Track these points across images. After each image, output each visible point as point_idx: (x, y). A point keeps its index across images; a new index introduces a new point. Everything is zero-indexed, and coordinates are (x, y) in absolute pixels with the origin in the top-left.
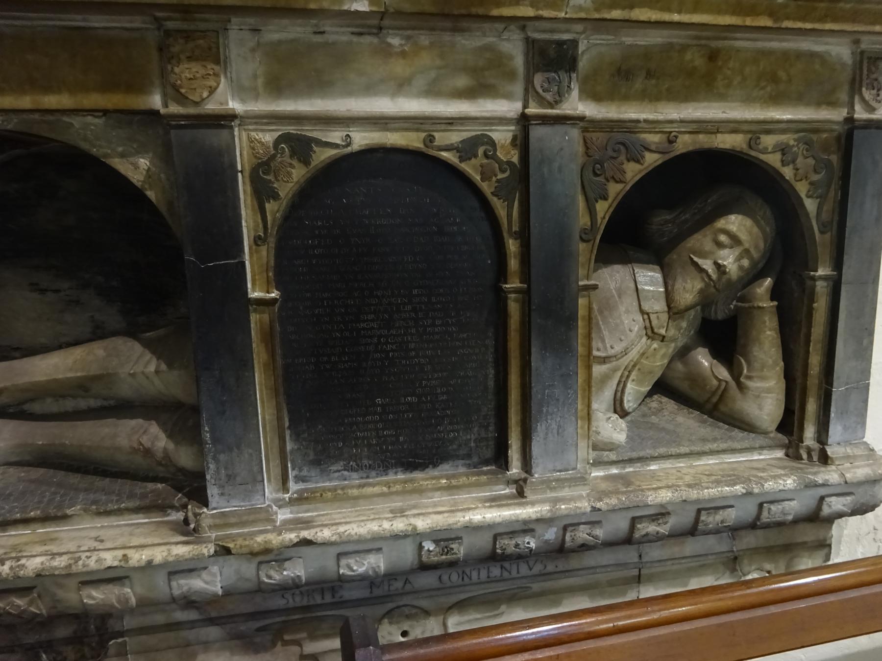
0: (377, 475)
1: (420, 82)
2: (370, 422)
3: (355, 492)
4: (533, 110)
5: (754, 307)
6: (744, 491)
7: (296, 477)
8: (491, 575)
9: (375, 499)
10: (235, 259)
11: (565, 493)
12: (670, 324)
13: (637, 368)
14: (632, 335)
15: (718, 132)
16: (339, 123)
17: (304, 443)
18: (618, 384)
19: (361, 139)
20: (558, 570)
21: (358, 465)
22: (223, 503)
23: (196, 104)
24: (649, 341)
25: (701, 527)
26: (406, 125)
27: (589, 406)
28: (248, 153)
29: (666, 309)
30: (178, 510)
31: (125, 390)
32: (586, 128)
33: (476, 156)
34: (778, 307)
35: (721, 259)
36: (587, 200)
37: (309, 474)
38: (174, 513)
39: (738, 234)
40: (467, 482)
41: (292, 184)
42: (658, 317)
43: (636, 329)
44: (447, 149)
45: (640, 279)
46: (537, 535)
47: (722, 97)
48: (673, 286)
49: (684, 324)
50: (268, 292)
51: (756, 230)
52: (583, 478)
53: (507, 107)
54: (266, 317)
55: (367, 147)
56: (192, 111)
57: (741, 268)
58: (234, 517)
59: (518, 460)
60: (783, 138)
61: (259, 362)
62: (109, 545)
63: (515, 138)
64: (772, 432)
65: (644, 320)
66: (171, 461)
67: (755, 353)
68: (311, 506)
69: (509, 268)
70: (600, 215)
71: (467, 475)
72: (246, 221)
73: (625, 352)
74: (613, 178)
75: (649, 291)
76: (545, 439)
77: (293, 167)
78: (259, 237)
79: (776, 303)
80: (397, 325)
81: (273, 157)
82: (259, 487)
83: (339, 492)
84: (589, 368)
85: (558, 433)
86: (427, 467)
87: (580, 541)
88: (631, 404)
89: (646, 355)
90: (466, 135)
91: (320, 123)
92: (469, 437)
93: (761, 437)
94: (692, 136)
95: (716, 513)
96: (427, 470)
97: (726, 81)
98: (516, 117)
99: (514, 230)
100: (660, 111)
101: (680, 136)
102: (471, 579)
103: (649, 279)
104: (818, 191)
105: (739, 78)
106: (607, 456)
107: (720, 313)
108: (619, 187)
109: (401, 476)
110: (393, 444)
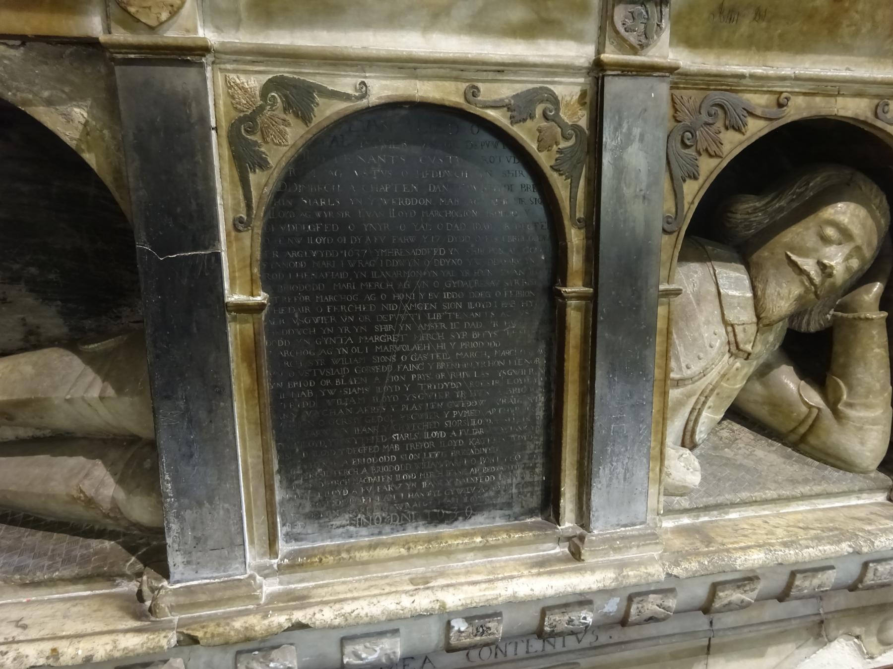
0: (393, 531)
1: (462, 13)
2: (385, 464)
3: (365, 555)
4: (610, 56)
5: (860, 319)
6: (851, 550)
7: (287, 534)
8: (531, 650)
9: (391, 563)
10: (206, 249)
11: (633, 554)
12: (758, 338)
13: (715, 392)
14: (713, 352)
15: (839, 94)
16: (352, 66)
17: (298, 491)
18: (691, 413)
19: (382, 88)
20: (612, 641)
21: (368, 519)
22: (189, 573)
23: (151, 29)
24: (732, 359)
25: (794, 592)
26: (442, 72)
27: (662, 444)
28: (225, 104)
29: (755, 320)
30: (130, 578)
31: (61, 420)
32: (676, 83)
33: (532, 117)
34: (888, 320)
35: (827, 258)
36: (672, 178)
37: (304, 531)
38: (125, 582)
39: (850, 227)
40: (507, 541)
41: (286, 148)
42: (744, 329)
43: (718, 344)
44: (495, 106)
45: (720, 282)
46: (595, 606)
47: (846, 49)
48: (764, 290)
49: (771, 338)
50: (252, 296)
51: (870, 222)
52: (654, 534)
53: (577, 52)
54: (249, 328)
55: (388, 101)
56: (145, 39)
57: (848, 269)
58: (204, 593)
59: (572, 511)
61: (240, 388)
62: (33, 634)
63: (583, 94)
64: (871, 471)
65: (727, 333)
66: (122, 513)
67: (859, 376)
68: (307, 575)
69: (569, 266)
70: (688, 198)
71: (507, 531)
72: (223, 198)
73: (704, 373)
74: (707, 150)
75: (733, 297)
76: (608, 486)
77: (289, 125)
78: (241, 220)
79: (884, 314)
80: (422, 338)
81: (261, 109)
82: (238, 552)
83: (344, 555)
84: (665, 394)
85: (625, 479)
86: (456, 520)
87: (647, 614)
88: (702, 436)
89: (727, 377)
90: (520, 88)
91: (325, 64)
92: (509, 481)
93: (860, 477)
94: (807, 98)
95: (814, 577)
96: (456, 523)
97: (853, 28)
98: (587, 65)
99: (578, 216)
100: (770, 64)
101: (792, 97)
102: (506, 655)
103: (733, 280)
105: (869, 25)
106: (678, 502)
107: (813, 324)
108: (714, 162)
109: (423, 532)
110: (413, 491)
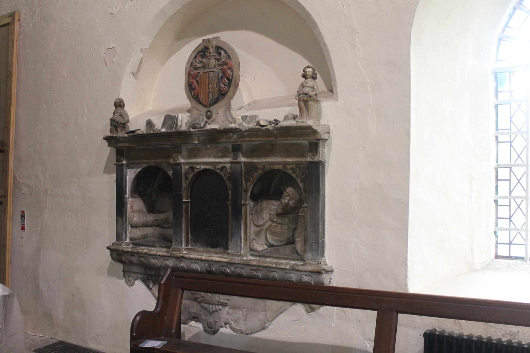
11: (235, 258)
19: (203, 167)
44: (218, 169)
47: (275, 156)
51: (295, 192)
60: (292, 166)
104: (304, 181)
